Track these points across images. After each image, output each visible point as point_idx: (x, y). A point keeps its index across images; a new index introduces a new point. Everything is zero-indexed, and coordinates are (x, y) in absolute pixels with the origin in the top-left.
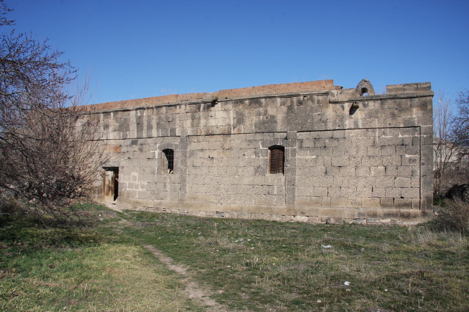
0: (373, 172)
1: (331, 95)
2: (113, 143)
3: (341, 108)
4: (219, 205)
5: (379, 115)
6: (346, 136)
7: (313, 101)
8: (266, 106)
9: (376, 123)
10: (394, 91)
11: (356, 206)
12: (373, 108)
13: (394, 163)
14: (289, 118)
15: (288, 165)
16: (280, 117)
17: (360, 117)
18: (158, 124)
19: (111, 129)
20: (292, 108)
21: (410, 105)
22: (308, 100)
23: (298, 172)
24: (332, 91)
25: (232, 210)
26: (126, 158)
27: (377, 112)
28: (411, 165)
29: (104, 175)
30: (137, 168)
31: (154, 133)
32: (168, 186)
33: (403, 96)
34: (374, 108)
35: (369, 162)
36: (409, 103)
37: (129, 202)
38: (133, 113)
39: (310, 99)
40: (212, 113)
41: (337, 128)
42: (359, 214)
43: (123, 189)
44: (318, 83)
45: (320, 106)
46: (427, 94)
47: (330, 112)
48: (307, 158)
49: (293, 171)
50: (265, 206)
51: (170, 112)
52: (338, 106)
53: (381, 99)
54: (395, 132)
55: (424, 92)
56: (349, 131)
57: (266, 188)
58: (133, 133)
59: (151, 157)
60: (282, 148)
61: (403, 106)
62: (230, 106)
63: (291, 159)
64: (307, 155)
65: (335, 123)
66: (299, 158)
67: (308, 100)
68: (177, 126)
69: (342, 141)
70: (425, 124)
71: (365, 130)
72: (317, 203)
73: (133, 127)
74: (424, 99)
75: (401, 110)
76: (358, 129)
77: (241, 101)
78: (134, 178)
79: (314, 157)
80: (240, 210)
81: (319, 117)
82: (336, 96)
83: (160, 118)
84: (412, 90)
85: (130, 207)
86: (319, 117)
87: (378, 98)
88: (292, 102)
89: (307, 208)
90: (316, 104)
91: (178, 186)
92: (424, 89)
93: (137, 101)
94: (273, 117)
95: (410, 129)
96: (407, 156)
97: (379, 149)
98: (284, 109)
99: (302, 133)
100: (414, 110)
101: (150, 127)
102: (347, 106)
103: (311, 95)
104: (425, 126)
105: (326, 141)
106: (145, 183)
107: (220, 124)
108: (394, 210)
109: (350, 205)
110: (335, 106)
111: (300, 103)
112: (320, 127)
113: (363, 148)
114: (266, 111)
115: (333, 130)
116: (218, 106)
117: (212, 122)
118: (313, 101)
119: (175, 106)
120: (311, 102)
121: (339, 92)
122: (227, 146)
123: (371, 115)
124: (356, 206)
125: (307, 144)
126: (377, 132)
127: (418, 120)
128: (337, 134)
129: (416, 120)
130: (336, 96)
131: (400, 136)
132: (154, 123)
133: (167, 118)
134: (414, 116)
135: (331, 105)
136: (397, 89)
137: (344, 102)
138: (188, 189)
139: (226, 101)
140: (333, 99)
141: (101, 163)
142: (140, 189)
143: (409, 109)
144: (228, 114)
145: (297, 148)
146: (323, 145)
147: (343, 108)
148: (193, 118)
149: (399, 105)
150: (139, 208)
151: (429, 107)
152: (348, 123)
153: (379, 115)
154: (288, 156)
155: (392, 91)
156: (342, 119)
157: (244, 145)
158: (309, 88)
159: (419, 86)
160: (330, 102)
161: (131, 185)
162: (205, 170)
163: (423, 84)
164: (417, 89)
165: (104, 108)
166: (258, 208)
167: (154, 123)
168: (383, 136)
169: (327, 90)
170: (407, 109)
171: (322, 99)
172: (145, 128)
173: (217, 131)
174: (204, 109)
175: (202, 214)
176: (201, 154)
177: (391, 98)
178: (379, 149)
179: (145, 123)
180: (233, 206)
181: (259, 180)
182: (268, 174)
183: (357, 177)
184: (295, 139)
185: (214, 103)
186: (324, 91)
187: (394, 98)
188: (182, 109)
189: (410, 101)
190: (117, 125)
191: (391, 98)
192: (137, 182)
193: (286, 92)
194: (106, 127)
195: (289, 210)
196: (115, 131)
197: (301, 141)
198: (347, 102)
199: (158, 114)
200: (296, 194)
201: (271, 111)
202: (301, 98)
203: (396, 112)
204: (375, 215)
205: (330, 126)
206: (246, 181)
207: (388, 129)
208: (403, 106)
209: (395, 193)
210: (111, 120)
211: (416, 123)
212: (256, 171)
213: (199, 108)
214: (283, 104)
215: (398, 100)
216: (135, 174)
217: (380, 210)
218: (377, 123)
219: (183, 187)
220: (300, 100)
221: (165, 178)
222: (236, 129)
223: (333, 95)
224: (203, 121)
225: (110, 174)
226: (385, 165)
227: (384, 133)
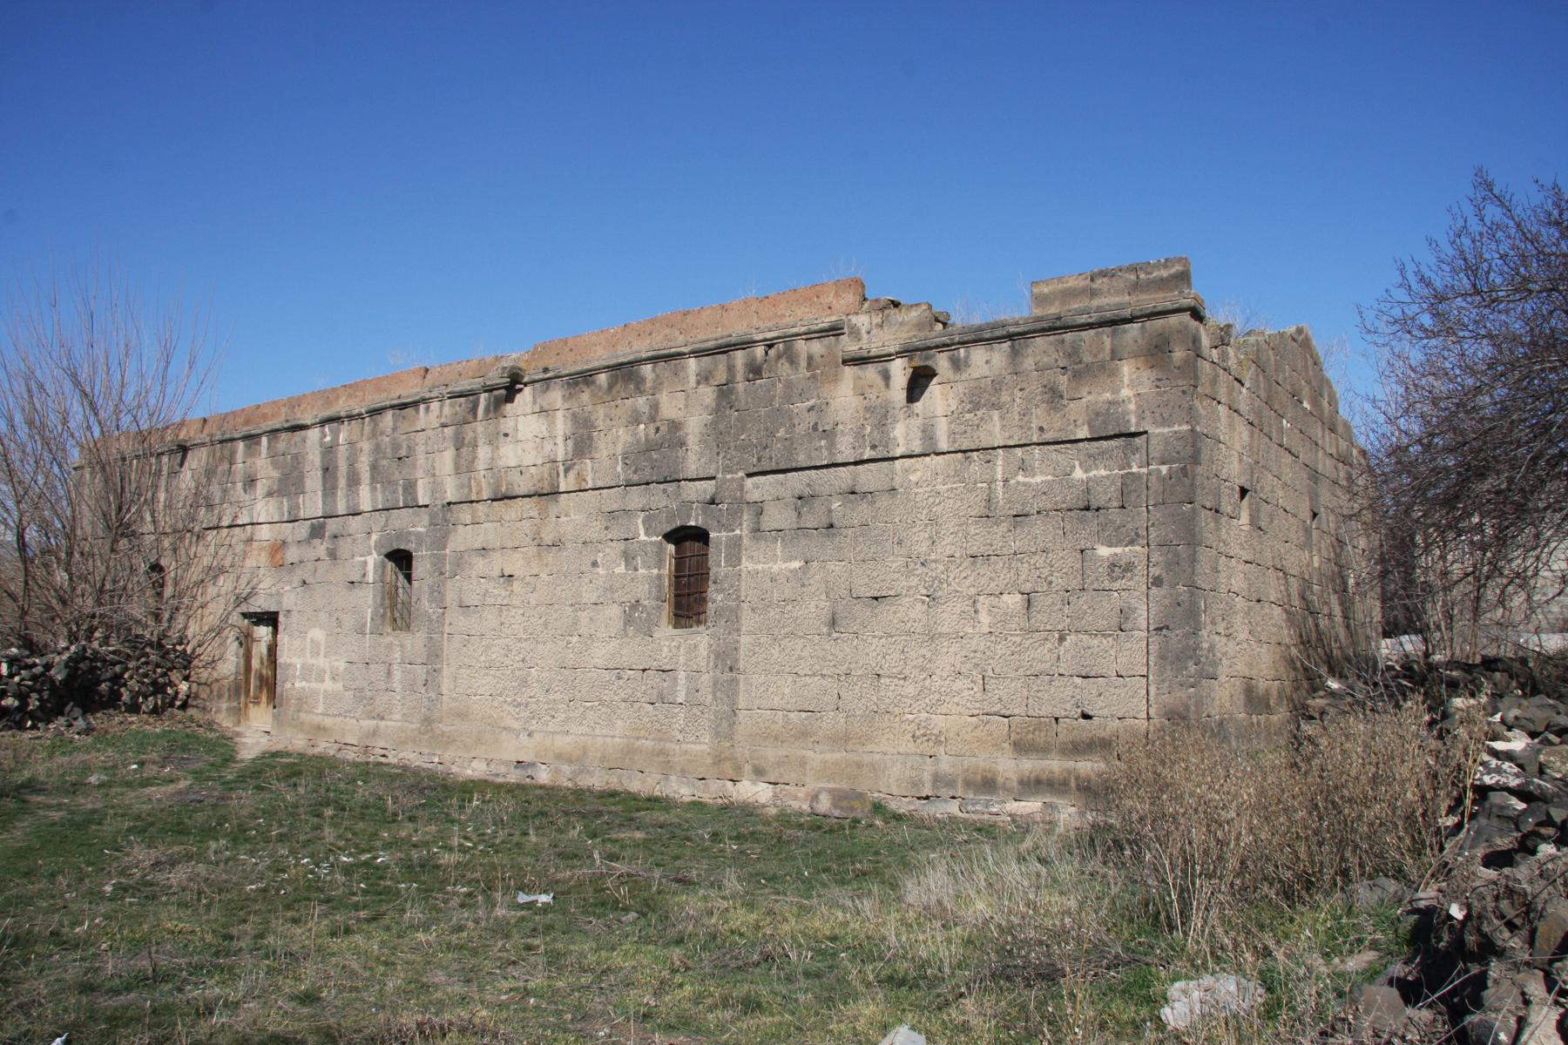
0: (984, 618)
2: (264, 533)
3: (879, 381)
4: (523, 737)
5: (1005, 397)
6: (896, 484)
7: (793, 361)
8: (656, 389)
9: (995, 431)
11: (928, 748)
12: (985, 371)
13: (1058, 581)
14: (721, 427)
15: (716, 597)
16: (695, 425)
17: (940, 411)
18: (374, 467)
20: (731, 391)
21: (1113, 351)
22: (779, 357)
23: (748, 621)
24: (854, 319)
25: (559, 756)
26: (296, 583)
27: (997, 385)
28: (1116, 585)
29: (246, 640)
30: (323, 616)
31: (365, 499)
32: (397, 674)
33: (1084, 319)
35: (971, 579)
36: (1107, 342)
37: (300, 726)
38: (313, 434)
39: (785, 352)
40: (507, 425)
42: (937, 779)
43: (288, 685)
45: (814, 377)
46: (1169, 305)
47: (845, 396)
48: (775, 568)
49: (732, 617)
50: (649, 743)
51: (404, 427)
52: (871, 372)
53: (1010, 337)
55: (1161, 295)
56: (908, 462)
57: (653, 679)
58: (312, 504)
59: (356, 578)
60: (701, 536)
61: (1087, 358)
62: (556, 396)
63: (726, 576)
64: (774, 558)
65: (859, 435)
66: (752, 568)
67: (779, 357)
68: (419, 474)
69: (883, 502)
70: (1164, 422)
71: (960, 455)
72: (804, 734)
73: (313, 481)
74: (1158, 323)
75: (1081, 372)
76: (938, 454)
77: (585, 378)
79: (796, 564)
80: (578, 759)
81: (812, 418)
83: (377, 449)
84: (1118, 292)
87: (998, 333)
88: (731, 369)
89: (771, 753)
90: (803, 372)
91: (420, 672)
92: (1162, 284)
93: (328, 396)
94: (675, 426)
95: (1113, 443)
96: (1104, 551)
97: (1004, 527)
98: (708, 394)
99: (762, 479)
100: (1127, 369)
101: (354, 481)
102: (900, 371)
103: (788, 339)
104: (1166, 430)
105: (835, 506)
106: (342, 665)
107: (529, 459)
108: (1055, 765)
109: (907, 746)
110: (861, 373)
111: (755, 371)
112: (814, 453)
113: (951, 526)
114: (655, 407)
116: (525, 397)
117: (510, 455)
118: (793, 361)
119: (415, 404)
120: (787, 365)
121: (877, 319)
122: (548, 538)
123: (980, 399)
124: (928, 748)
125: (776, 517)
126: (1000, 462)
127: (1139, 407)
128: (869, 477)
129: (1132, 407)
130: (865, 336)
131: (1079, 474)
133: (396, 446)
134: (1126, 392)
135: (849, 371)
136: (1069, 294)
138: (446, 685)
139: (546, 381)
141: (241, 600)
142: (328, 685)
143: (1104, 369)
144: (552, 425)
145: (745, 532)
146: (825, 521)
147: (886, 377)
148: (459, 444)
149: (1074, 353)
150: (324, 747)
151: (1179, 354)
152: (903, 435)
154: (718, 564)
155: (1051, 304)
156: (882, 417)
157: (595, 530)
158: (783, 316)
159: (1142, 276)
160: (845, 362)
161: (307, 672)
162: (491, 618)
163: (1158, 266)
164: (1136, 287)
165: (247, 422)
166: (630, 751)
168: (1020, 478)
169: (834, 318)
170: (1103, 367)
172: (342, 482)
173: (523, 486)
174: (487, 411)
175: (475, 770)
176: (480, 564)
177: (1044, 331)
178: (1004, 527)
180: (562, 743)
181: (633, 651)
182: (665, 631)
183: (932, 637)
184: (740, 502)
185: (512, 386)
186: (826, 321)
187: (1054, 328)
188: (429, 418)
189: (1114, 335)
190: (276, 474)
191: (1044, 330)
192: (322, 662)
193: (709, 335)
194: (250, 482)
195: (718, 760)
196: (270, 494)
197: (759, 509)
200: (742, 704)
201: (670, 406)
202: (759, 351)
204: (988, 784)
205: (845, 452)
206: (599, 654)
207: (1037, 450)
208: (1087, 358)
209: (1060, 698)
211: (1133, 420)
212: (628, 621)
213: (474, 410)
214: (704, 378)
215: (1068, 337)
216: (317, 634)
217: (1009, 767)
218: (997, 430)
219: (432, 679)
220: (754, 359)
221: (390, 646)
222: (572, 475)
223: (855, 333)
224: (483, 452)
225: (263, 632)
226: (1027, 587)
227: (1023, 467)
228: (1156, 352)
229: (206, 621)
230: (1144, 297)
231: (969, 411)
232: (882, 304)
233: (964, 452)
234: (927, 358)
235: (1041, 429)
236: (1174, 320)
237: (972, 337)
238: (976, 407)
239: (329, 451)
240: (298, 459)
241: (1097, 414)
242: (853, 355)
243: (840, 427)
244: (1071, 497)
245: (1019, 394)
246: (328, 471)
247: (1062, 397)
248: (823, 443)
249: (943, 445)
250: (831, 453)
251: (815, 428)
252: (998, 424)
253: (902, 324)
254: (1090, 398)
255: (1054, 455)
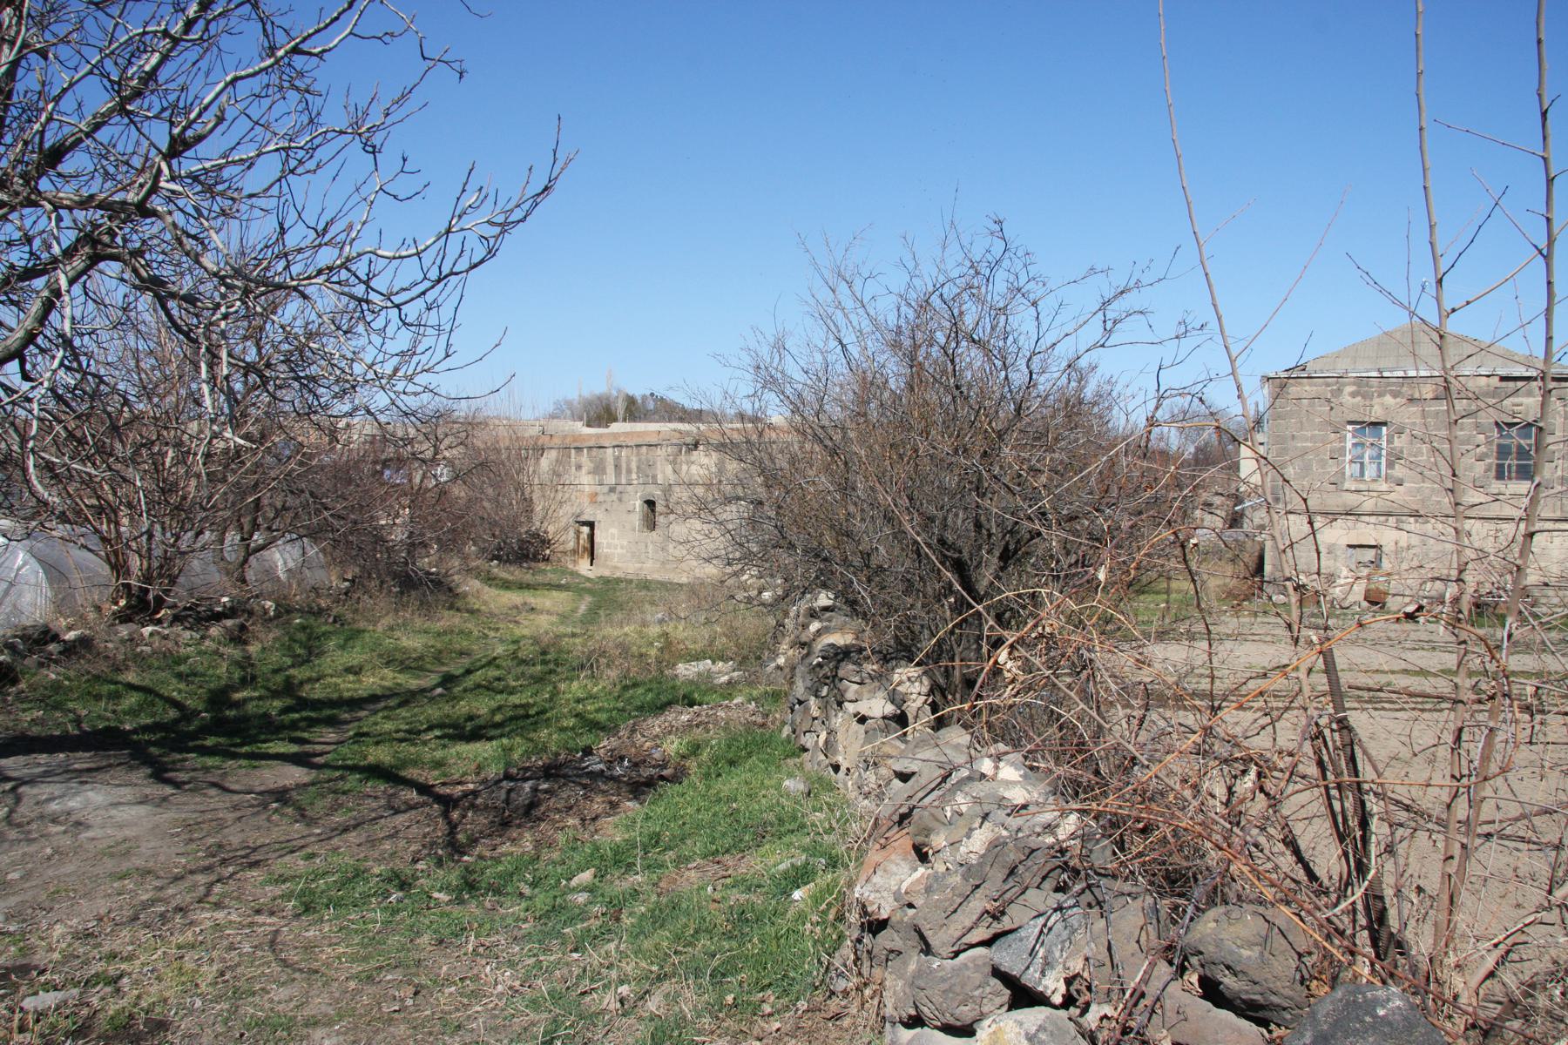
2: (587, 489)
19: (584, 470)
29: (578, 533)
38: (610, 451)
58: (610, 478)
73: (610, 469)
78: (613, 536)
85: (607, 573)
101: (629, 471)
132: (634, 466)
142: (619, 550)
150: (618, 574)
161: (609, 546)
167: (634, 466)
179: (624, 466)
185: (696, 445)
194: (579, 467)
199: (638, 454)
210: (584, 458)
216: (613, 531)
224: (685, 467)
225: (586, 530)
229: (558, 526)
239: (617, 459)
240: (602, 461)
246: (617, 467)
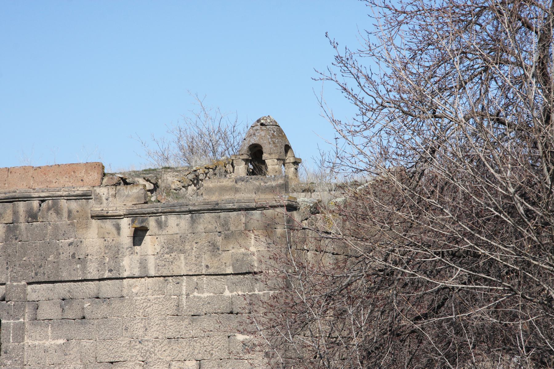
1: (96, 199)
5: (187, 247)
6: (125, 293)
7: (58, 212)
9: (182, 266)
10: (217, 194)
12: (175, 230)
13: (217, 354)
14: (9, 251)
17: (150, 252)
20: (16, 228)
22: (49, 209)
27: (183, 239)
28: (247, 356)
34: (178, 232)
35: (168, 352)
36: (243, 220)
41: (107, 275)
44: (71, 169)
45: (72, 224)
47: (93, 237)
48: (47, 343)
52: (108, 224)
53: (190, 212)
54: (218, 283)
61: (232, 228)
63: (14, 349)
64: (46, 337)
65: (102, 263)
67: (49, 209)
69: (116, 304)
71: (162, 278)
74: (270, 212)
76: (149, 277)
79: (61, 341)
81: (72, 250)
82: (105, 201)
86: (72, 250)
87: (183, 209)
88: (15, 213)
90: (65, 220)
96: (240, 337)
97: (186, 322)
99: (38, 286)
103: (55, 198)
105: (86, 305)
110: (103, 225)
111: (32, 216)
112: (73, 272)
113: (156, 320)
115: (99, 280)
118: (58, 212)
120: (54, 215)
121: (112, 191)
123: (173, 247)
125: (48, 311)
126: (184, 284)
128: (107, 288)
130: (105, 201)
131: (227, 293)
135: (95, 223)
137: (119, 217)
140: (97, 209)
145: (27, 320)
146: (80, 315)
147: (118, 228)
149: (225, 225)
151: (280, 230)
152: (128, 264)
153: (187, 247)
156: (116, 253)
158: (51, 182)
160: (92, 217)
168: (196, 294)
169: (85, 189)
171: (78, 208)
178: (186, 322)
186: (80, 190)
187: (215, 209)
191: (209, 210)
198: (126, 216)
203: (219, 240)
205: (93, 272)
207: (205, 278)
215: (222, 214)
218: (183, 265)
220: (32, 209)
223: (98, 199)
226: (199, 357)
228: (268, 228)
230: (263, 196)
231: (167, 253)
232: (115, 181)
233: (164, 277)
234: (143, 222)
235: (207, 266)
236: (278, 210)
237: (169, 210)
238: (171, 251)
241: (237, 260)
242: (97, 213)
243: (89, 257)
244: (224, 307)
245: (195, 245)
247: (218, 249)
248: (78, 266)
249: (152, 272)
250: (84, 273)
251: (73, 256)
252: (183, 262)
253: (128, 196)
254: (233, 251)
255: (214, 281)
